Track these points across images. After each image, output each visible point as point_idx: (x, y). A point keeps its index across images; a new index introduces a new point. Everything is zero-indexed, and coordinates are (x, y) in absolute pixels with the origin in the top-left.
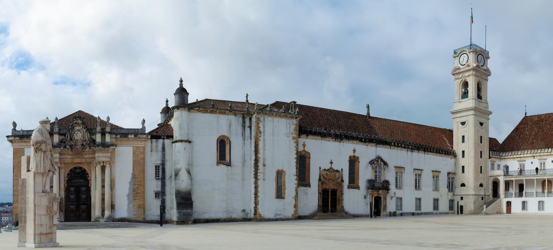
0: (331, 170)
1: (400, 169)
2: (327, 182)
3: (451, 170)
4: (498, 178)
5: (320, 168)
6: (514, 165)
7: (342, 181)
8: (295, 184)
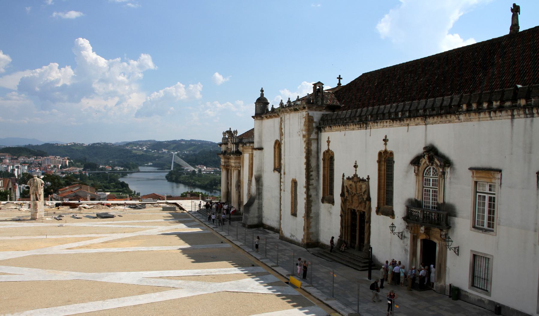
0: (355, 179)
1: (486, 173)
2: (349, 198)
5: (343, 176)
7: (369, 199)
8: (305, 199)
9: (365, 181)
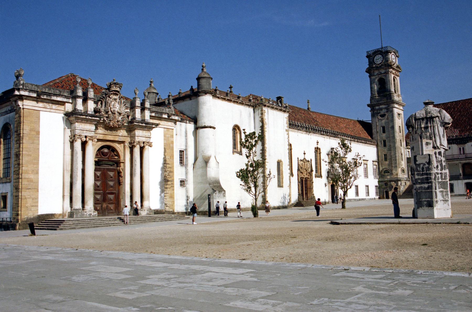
0: (304, 160)
5: (298, 159)
7: (312, 171)
9: (309, 161)
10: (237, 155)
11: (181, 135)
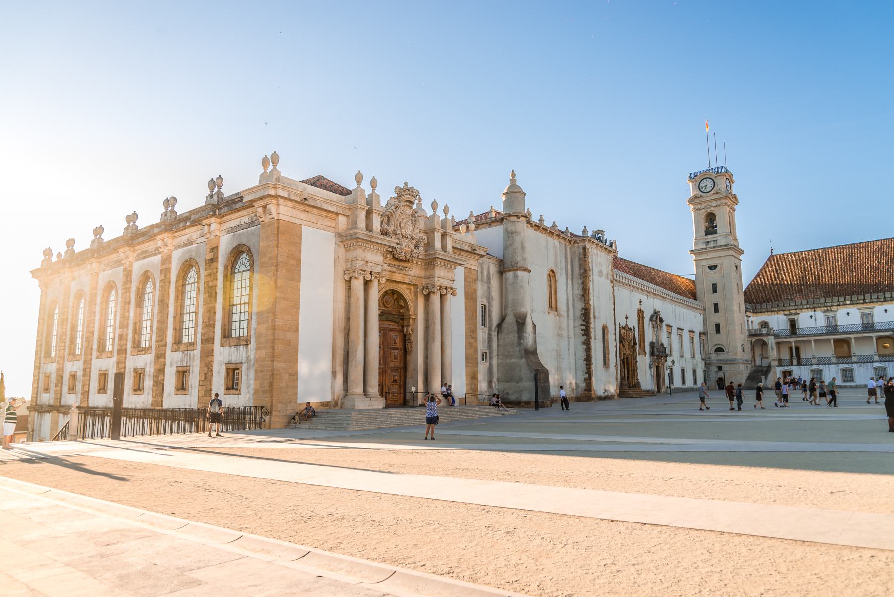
0: (626, 328)
3: (702, 330)
4: (765, 339)
6: (778, 321)
7: (635, 344)
10: (553, 313)
11: (482, 280)
